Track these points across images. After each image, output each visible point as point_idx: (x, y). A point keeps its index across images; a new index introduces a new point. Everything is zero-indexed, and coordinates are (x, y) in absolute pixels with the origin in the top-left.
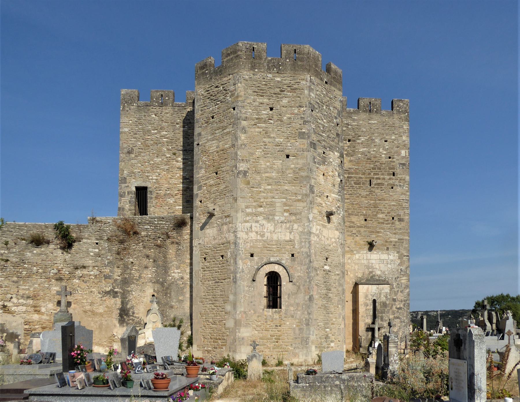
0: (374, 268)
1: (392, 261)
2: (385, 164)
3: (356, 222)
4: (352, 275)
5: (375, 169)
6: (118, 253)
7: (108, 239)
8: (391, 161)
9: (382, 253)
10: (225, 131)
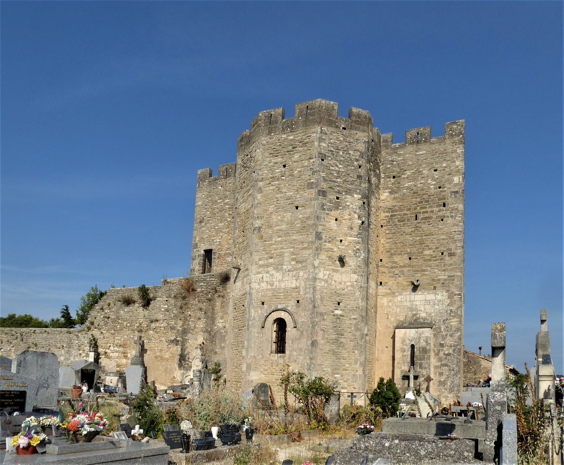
0: (418, 311)
2: (434, 195)
3: (398, 262)
4: (392, 319)
5: (422, 202)
6: (181, 308)
7: (175, 296)
8: (441, 191)
9: (428, 294)
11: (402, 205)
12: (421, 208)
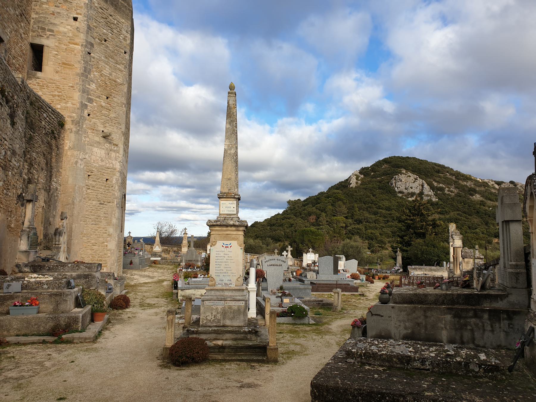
10: (118, 66)
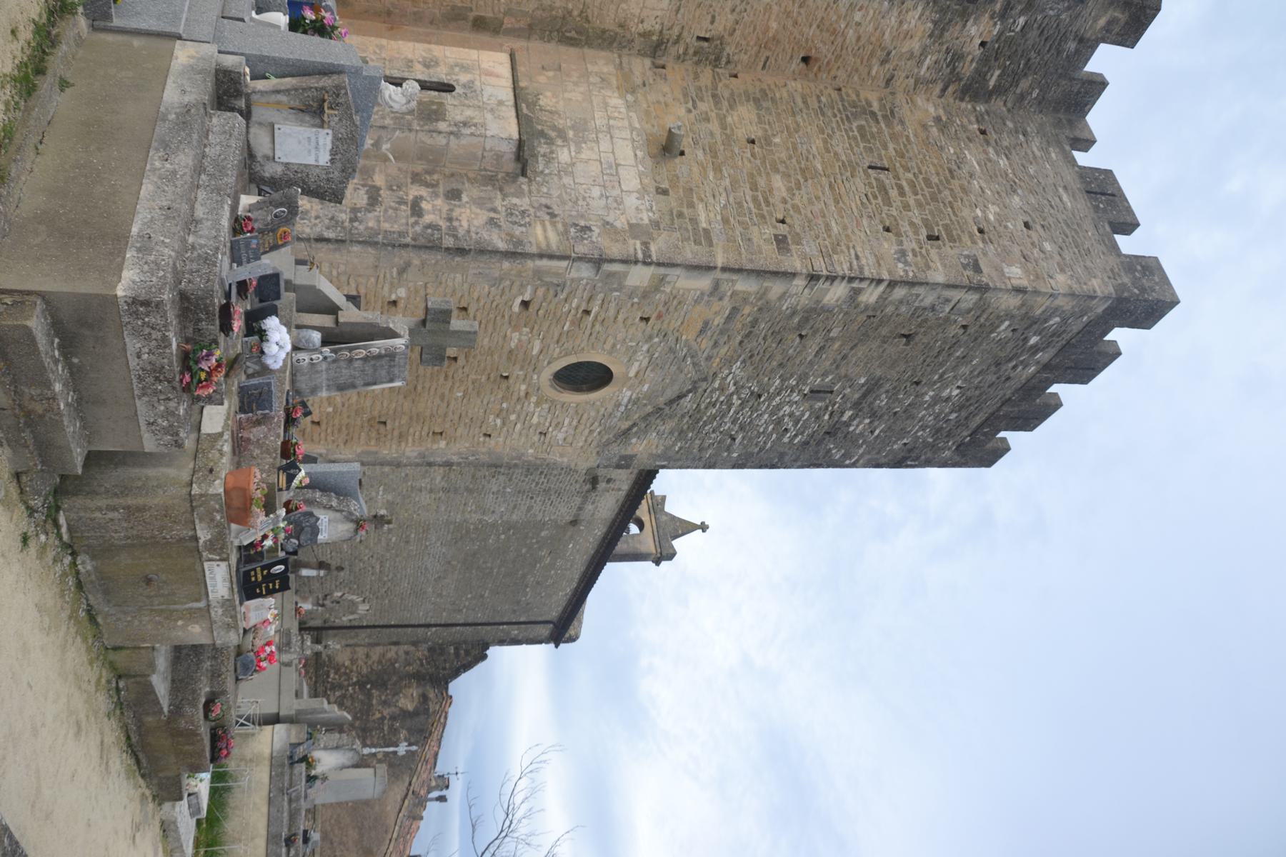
0: (578, 145)
1: (619, 202)
2: (956, 215)
9: (641, 175)
11: (908, 137)
12: (912, 185)
